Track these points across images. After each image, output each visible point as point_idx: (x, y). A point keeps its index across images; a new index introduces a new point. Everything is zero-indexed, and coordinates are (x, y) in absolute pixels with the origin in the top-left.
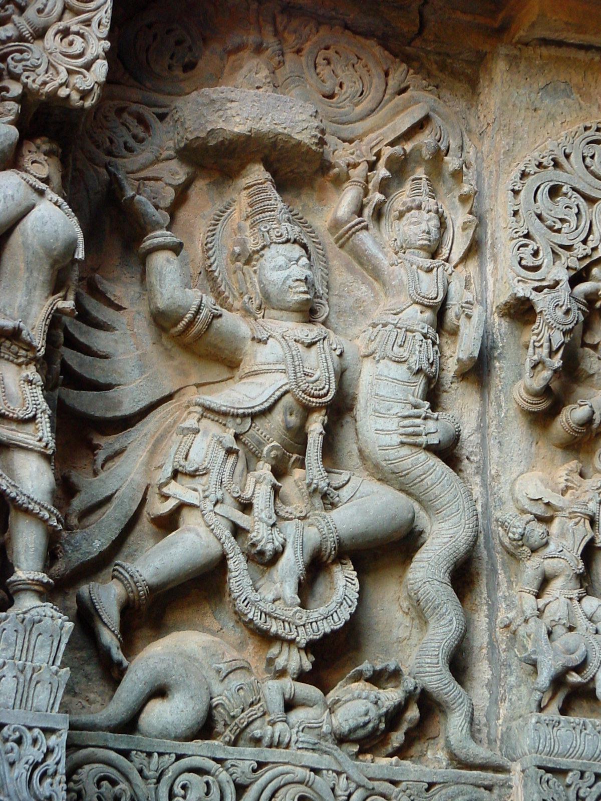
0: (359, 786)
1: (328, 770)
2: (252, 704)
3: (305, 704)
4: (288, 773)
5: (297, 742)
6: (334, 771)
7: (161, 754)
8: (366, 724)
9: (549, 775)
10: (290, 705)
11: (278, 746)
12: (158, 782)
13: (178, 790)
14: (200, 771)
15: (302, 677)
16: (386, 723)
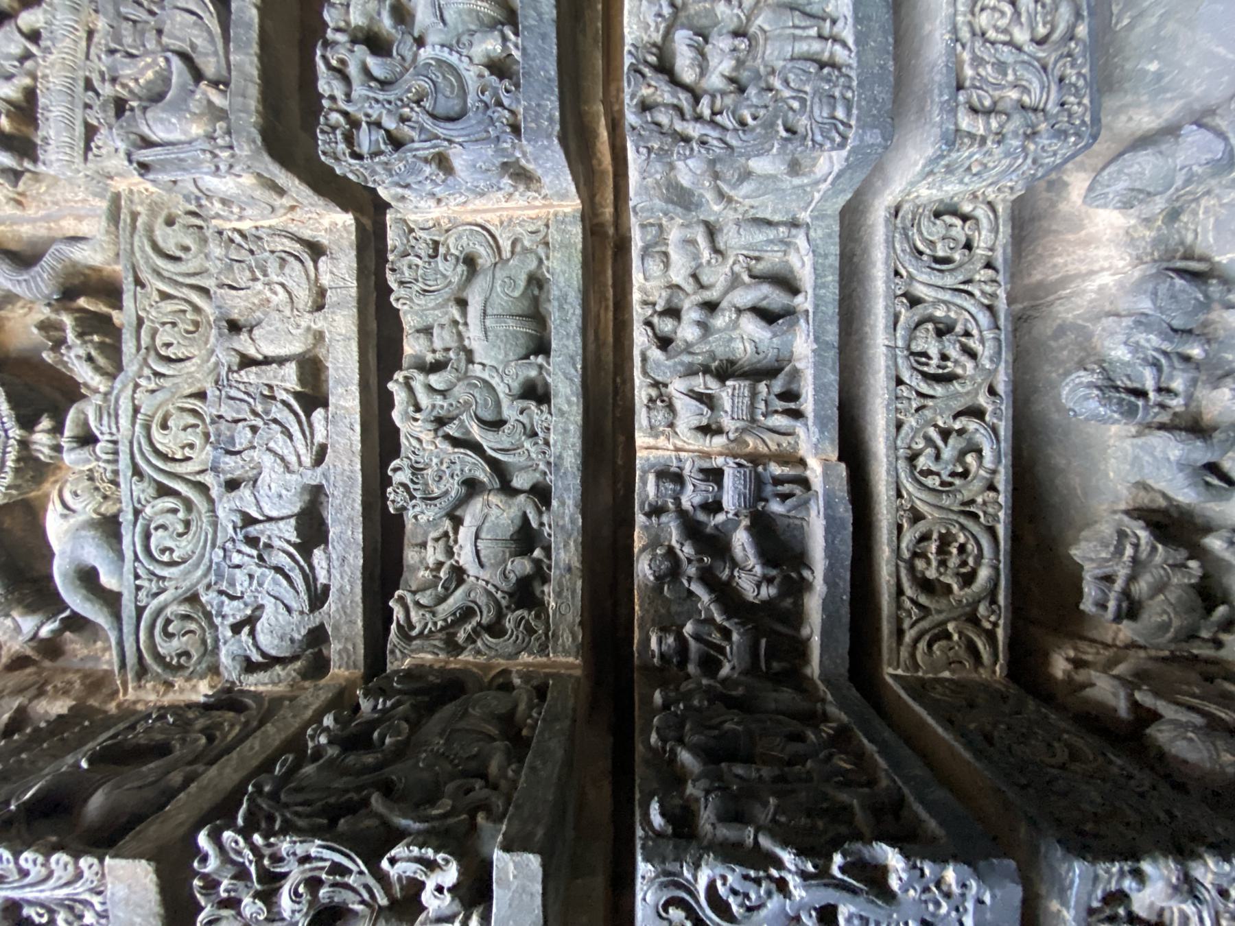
0: (145, 362)
1: (133, 399)
2: (91, 479)
3: (86, 423)
4: (140, 444)
5: (111, 434)
6: (134, 392)
7: (137, 577)
8: (90, 359)
9: (93, 145)
10: (87, 439)
11: (116, 453)
12: (163, 578)
13: (166, 558)
14: (147, 536)
15: (58, 429)
16: (91, 334)
